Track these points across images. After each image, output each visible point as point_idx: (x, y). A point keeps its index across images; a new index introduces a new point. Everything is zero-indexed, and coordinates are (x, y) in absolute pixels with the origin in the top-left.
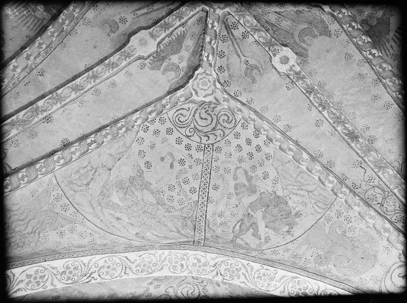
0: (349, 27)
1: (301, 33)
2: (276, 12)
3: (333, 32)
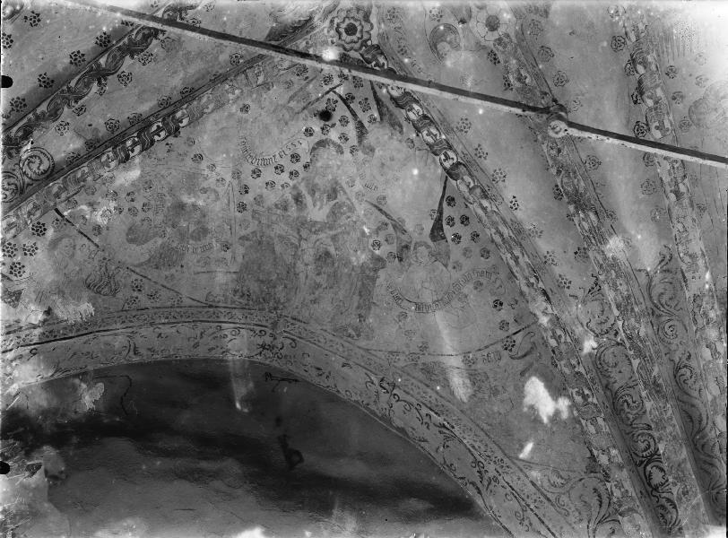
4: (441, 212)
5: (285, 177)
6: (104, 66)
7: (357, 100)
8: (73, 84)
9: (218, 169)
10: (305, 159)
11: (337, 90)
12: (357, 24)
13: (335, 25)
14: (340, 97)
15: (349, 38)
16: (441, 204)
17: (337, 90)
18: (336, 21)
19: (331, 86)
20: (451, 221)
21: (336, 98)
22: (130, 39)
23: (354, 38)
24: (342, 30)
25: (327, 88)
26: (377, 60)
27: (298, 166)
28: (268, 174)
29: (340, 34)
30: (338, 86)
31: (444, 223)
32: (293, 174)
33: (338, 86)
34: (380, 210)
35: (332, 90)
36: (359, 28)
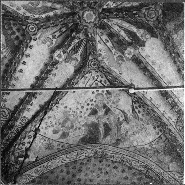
0: (13, 16)
1: (38, 4)
2: (57, 9)
3: (22, 8)
4: (133, 106)
5: (90, 106)
7: (103, 81)
8: (27, 99)
9: (72, 109)
10: (94, 100)
11: (97, 80)
12: (95, 62)
13: (90, 64)
14: (99, 81)
15: (94, 67)
16: (132, 104)
17: (97, 80)
18: (90, 63)
19: (95, 79)
20: (136, 108)
21: (98, 82)
22: (38, 84)
23: (96, 66)
24: (92, 65)
25: (94, 80)
26: (103, 70)
27: (93, 102)
28: (86, 107)
29: (92, 66)
30: (97, 79)
31: (135, 109)
32: (92, 105)
33: (97, 79)
34: (117, 108)
35: (96, 80)
36: (96, 63)
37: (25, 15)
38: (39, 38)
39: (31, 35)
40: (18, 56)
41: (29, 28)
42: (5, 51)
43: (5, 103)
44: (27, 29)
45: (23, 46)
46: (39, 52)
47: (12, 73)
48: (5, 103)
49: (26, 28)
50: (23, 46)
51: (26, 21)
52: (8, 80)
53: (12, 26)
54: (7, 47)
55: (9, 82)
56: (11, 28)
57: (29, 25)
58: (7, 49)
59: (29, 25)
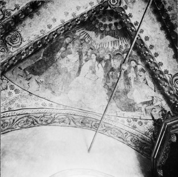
0: (94, 10)
6: (175, 38)
22: (169, 28)
37: (99, 2)
38: (126, 3)
39: (119, 7)
40: (131, 31)
41: (111, 4)
42: (122, 42)
43: (169, 73)
44: (112, 6)
45: (125, 20)
46: (139, 11)
47: (143, 46)
48: (169, 73)
49: (110, 7)
50: (125, 20)
51: (104, 2)
52: (147, 54)
53: (104, 23)
54: (118, 38)
55: (150, 54)
56: (106, 26)
57: (109, 2)
58: (121, 40)
59: (109, 2)
